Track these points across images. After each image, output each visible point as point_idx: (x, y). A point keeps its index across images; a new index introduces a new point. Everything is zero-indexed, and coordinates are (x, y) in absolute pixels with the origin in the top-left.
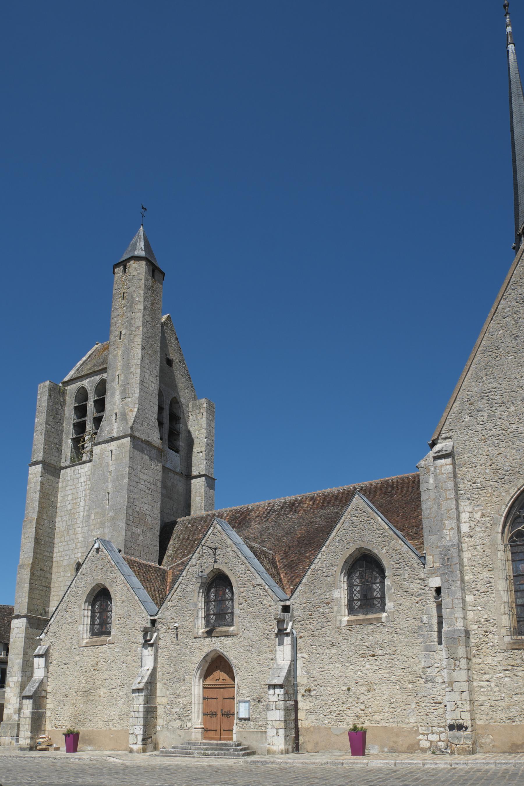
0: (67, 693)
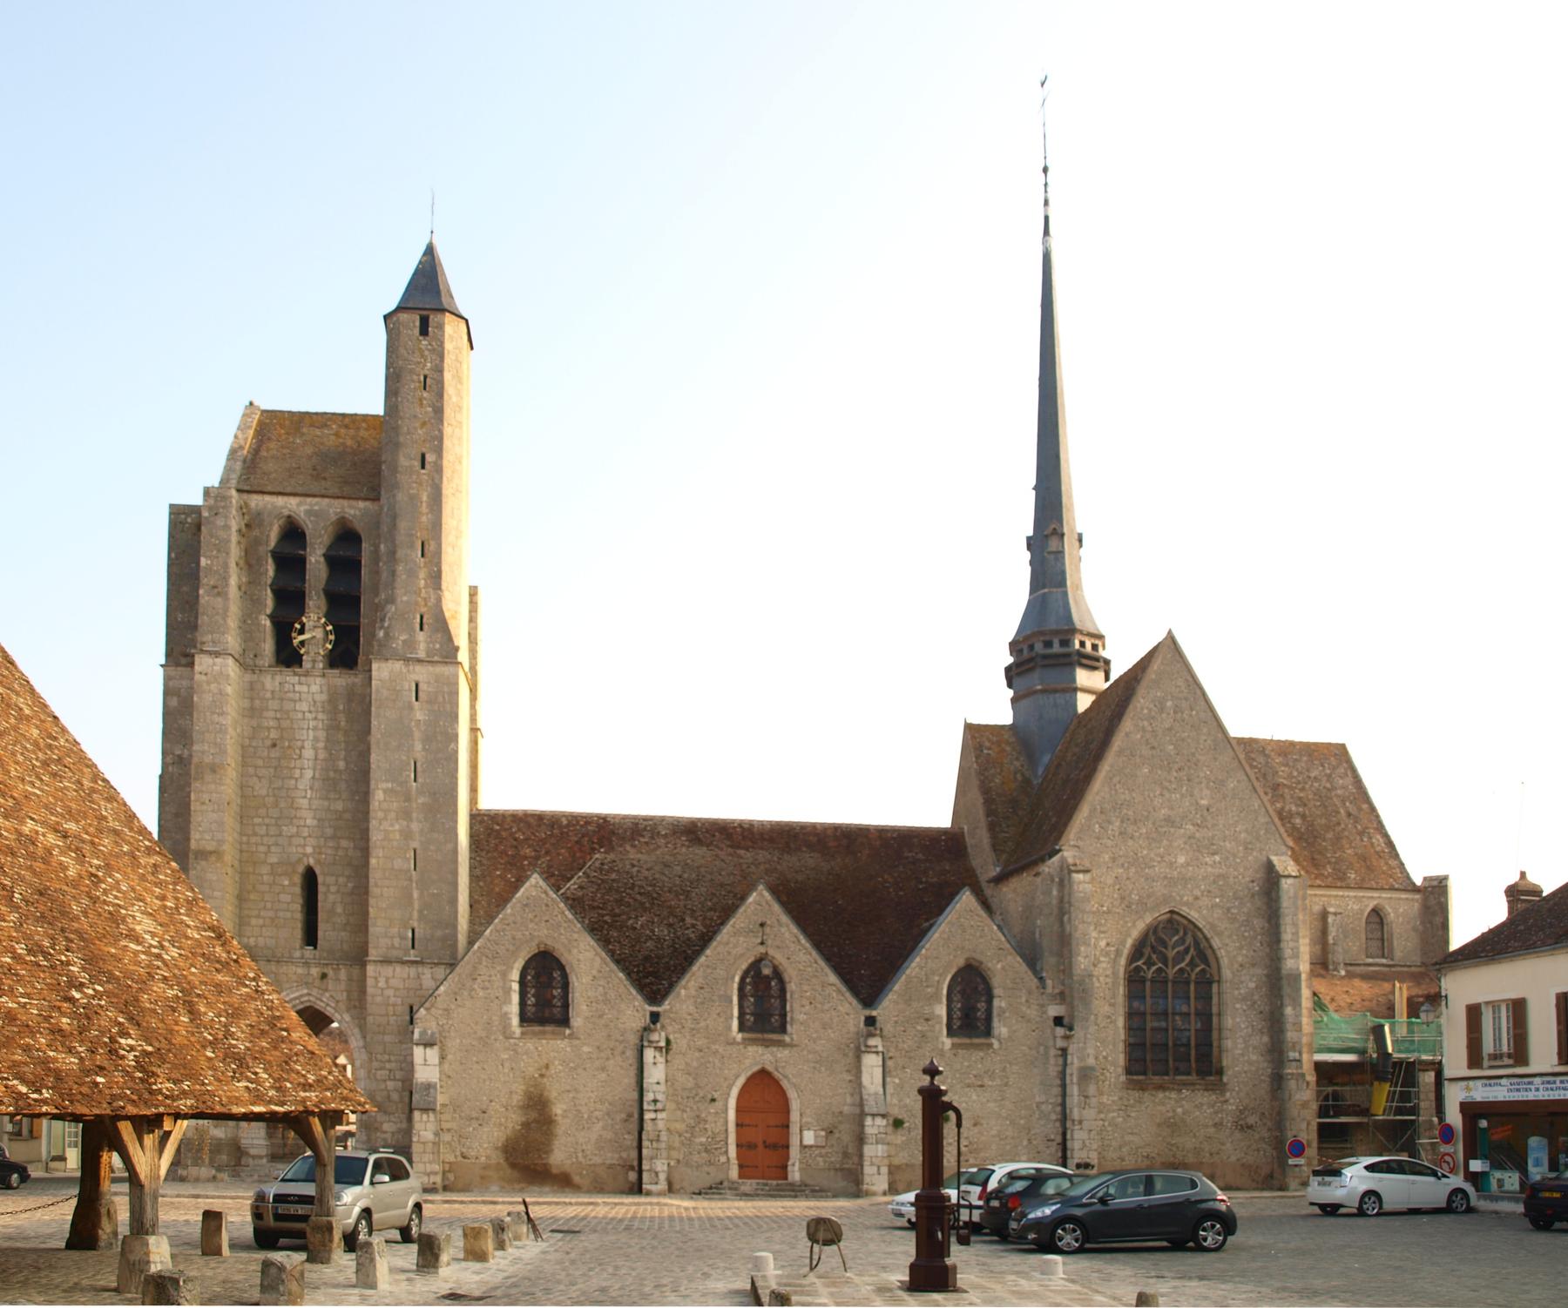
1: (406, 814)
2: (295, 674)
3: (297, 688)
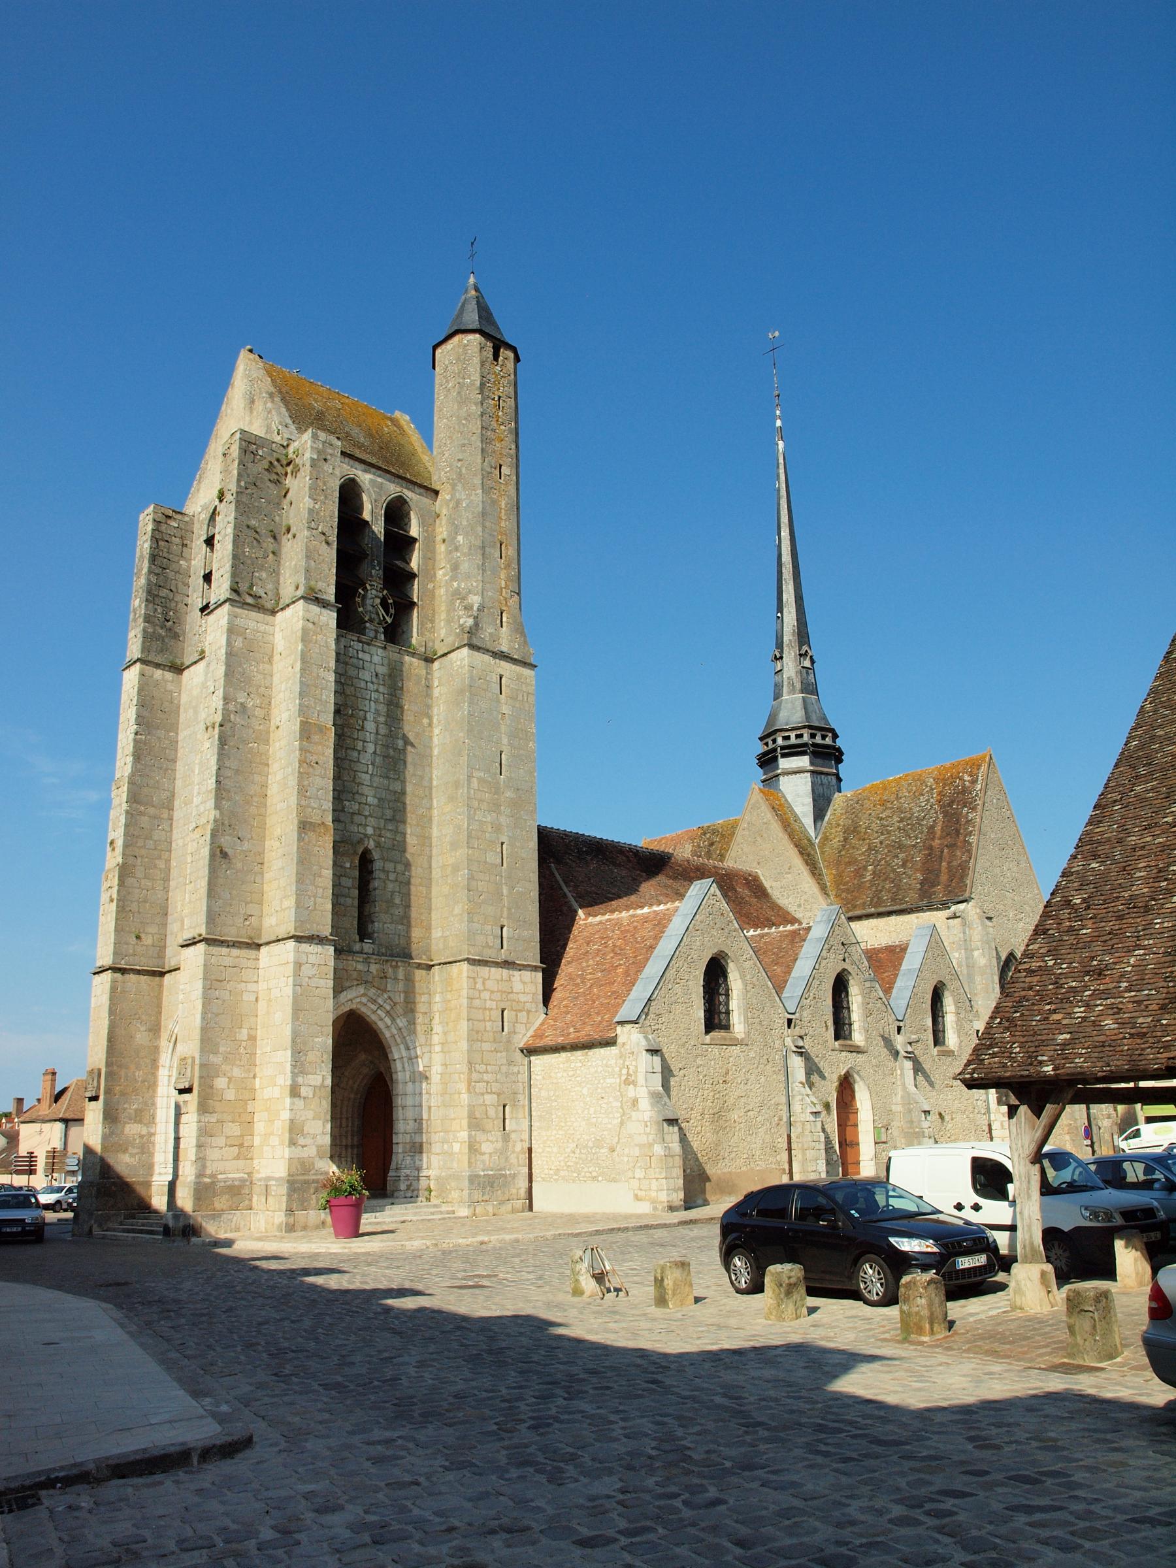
1: (495, 807)
2: (359, 641)
3: (361, 655)
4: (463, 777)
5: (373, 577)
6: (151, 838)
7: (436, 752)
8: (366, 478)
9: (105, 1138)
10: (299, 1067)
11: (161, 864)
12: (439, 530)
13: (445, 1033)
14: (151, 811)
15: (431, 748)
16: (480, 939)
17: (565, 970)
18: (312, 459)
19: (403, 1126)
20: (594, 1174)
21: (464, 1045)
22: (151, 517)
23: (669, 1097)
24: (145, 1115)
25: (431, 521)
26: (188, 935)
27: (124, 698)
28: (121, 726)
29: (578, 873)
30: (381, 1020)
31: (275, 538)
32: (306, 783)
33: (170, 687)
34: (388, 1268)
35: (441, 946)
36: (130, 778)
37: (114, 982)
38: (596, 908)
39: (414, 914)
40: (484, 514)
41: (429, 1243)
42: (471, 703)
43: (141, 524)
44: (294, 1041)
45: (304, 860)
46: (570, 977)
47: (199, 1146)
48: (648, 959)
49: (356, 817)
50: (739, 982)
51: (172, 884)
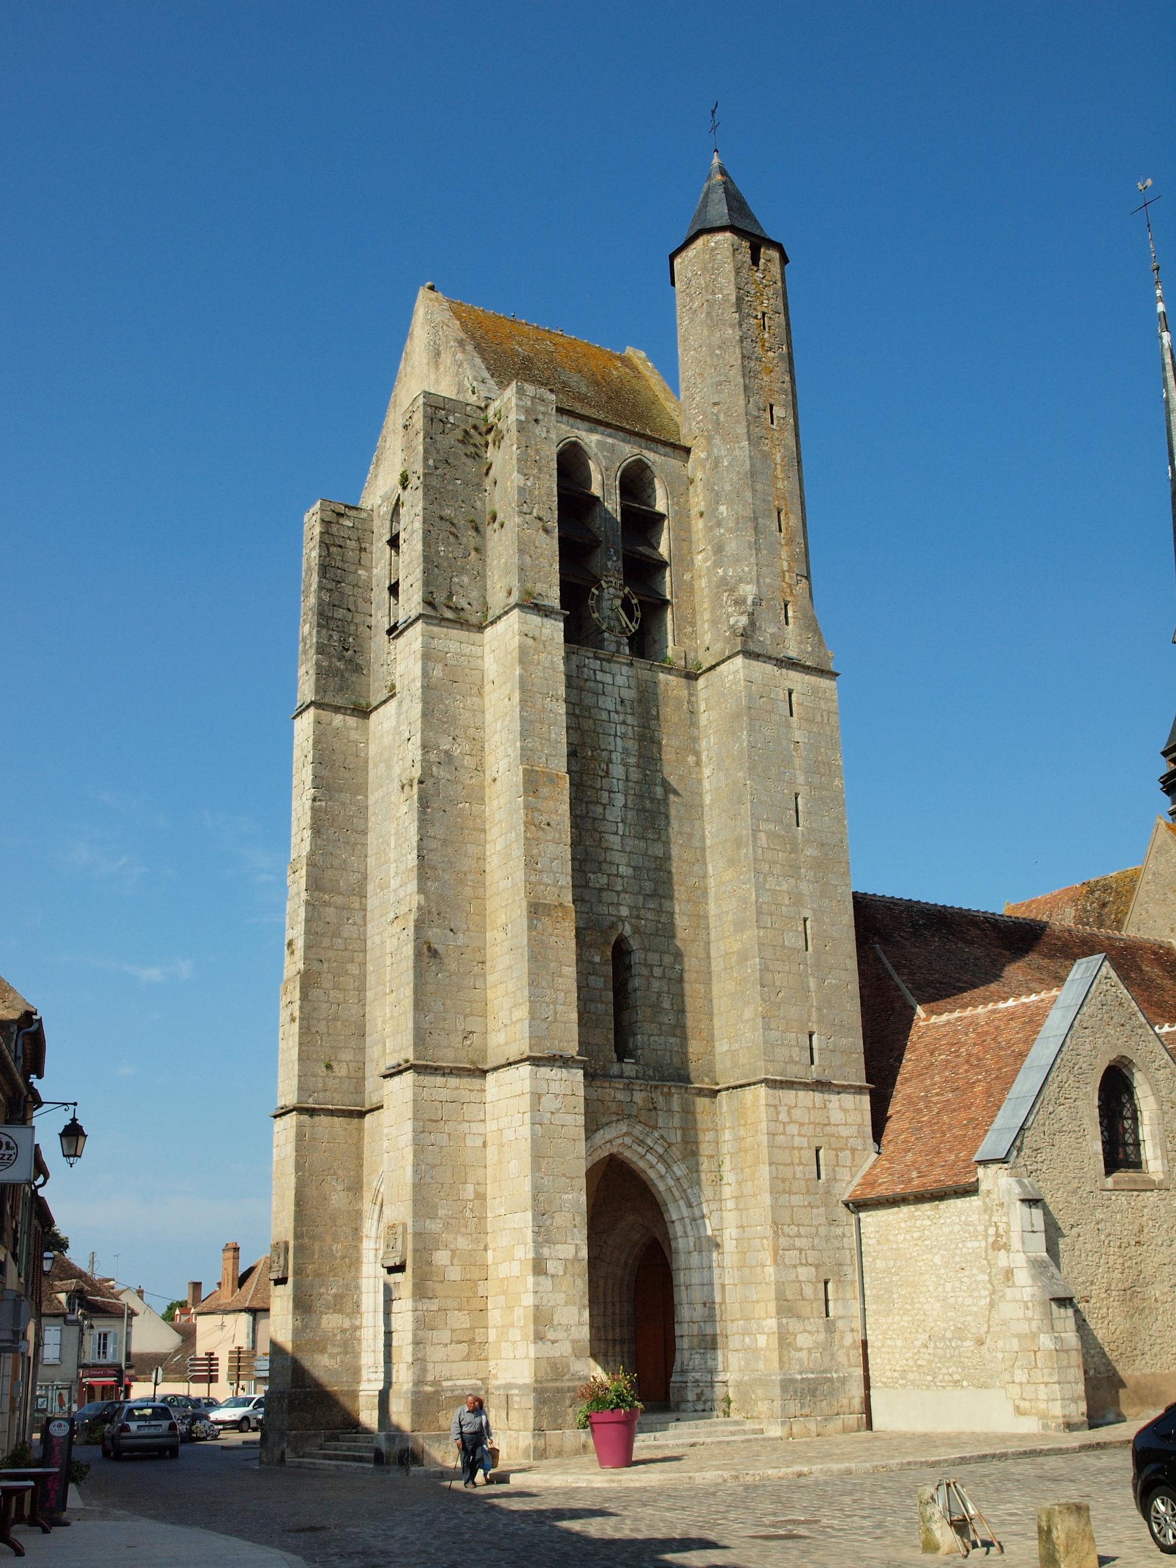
0: (1086, 1293)
1: (793, 870)
2: (596, 658)
4: (746, 832)
5: (609, 573)
6: (337, 934)
7: (707, 799)
8: (591, 440)
9: (296, 1332)
10: (543, 1234)
11: (354, 969)
12: (693, 500)
13: (739, 1183)
14: (339, 900)
15: (701, 795)
16: (781, 1053)
17: (903, 1091)
18: (519, 422)
19: (688, 1312)
20: (957, 1377)
21: (766, 1199)
22: (317, 517)
23: (1058, 1266)
24: (346, 1302)
25: (683, 489)
26: (391, 1061)
27: (297, 754)
28: (294, 791)
29: (913, 957)
30: (652, 1167)
31: (477, 530)
32: (535, 852)
33: (354, 735)
34: (669, 1509)
35: (728, 1063)
36: (309, 858)
37: (300, 1126)
38: (941, 1003)
39: (690, 1022)
40: (753, 474)
41: (726, 1475)
42: (751, 731)
43: (306, 527)
44: (535, 1199)
45: (538, 956)
46: (909, 1101)
47: (417, 1343)
48: (1017, 1071)
49: (604, 894)
50: (1151, 1099)
51: (370, 995)
